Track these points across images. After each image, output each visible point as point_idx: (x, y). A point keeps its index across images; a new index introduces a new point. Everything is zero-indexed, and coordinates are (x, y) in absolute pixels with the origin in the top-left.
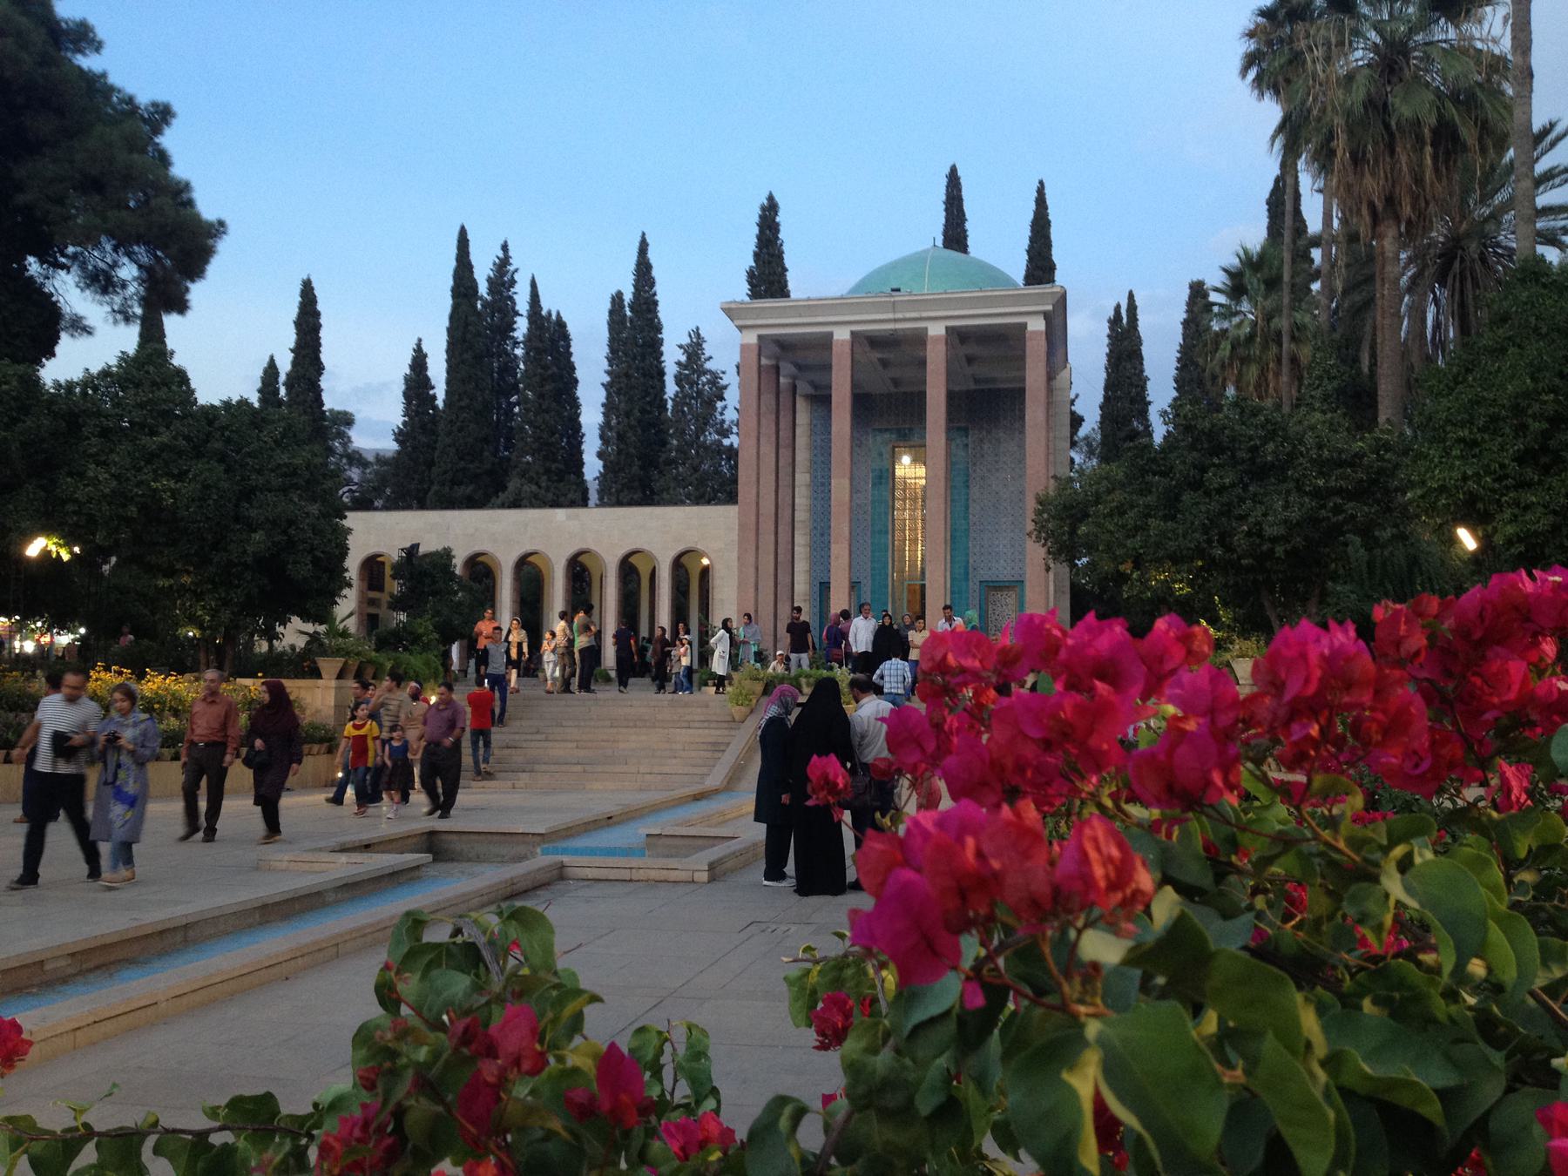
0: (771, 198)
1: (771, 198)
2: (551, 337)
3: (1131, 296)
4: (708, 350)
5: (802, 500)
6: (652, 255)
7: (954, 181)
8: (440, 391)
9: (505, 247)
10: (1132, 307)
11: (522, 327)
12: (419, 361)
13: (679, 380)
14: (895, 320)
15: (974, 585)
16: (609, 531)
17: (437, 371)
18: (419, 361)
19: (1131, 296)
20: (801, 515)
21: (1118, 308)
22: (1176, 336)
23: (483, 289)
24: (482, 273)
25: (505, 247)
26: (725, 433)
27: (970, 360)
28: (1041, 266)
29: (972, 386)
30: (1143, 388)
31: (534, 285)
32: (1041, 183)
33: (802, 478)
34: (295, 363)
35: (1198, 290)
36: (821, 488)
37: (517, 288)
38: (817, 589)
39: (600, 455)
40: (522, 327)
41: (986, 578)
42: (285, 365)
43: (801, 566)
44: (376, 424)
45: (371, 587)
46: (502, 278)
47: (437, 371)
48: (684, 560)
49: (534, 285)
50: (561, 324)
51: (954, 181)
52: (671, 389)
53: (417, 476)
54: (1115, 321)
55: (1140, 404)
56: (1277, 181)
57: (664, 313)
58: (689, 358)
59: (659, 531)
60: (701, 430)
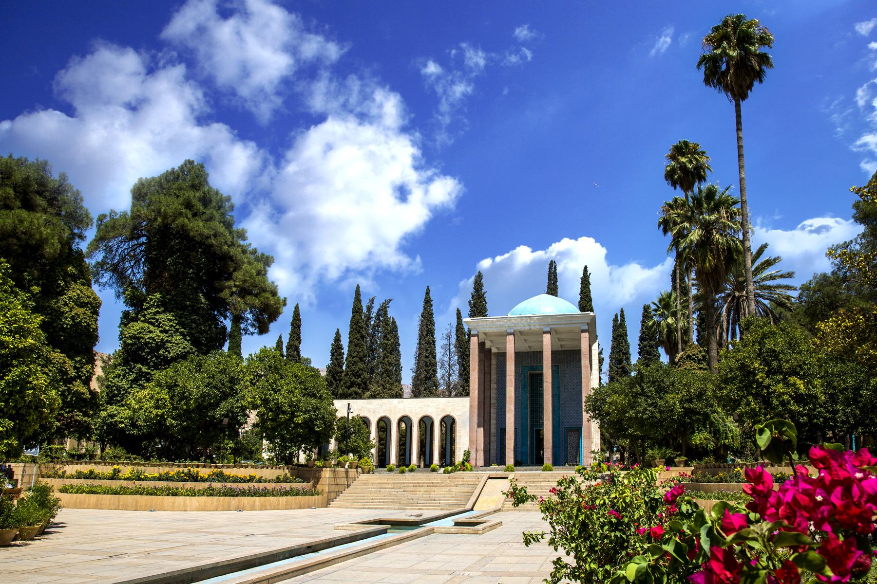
3: (622, 311)
5: (494, 394)
6: (431, 295)
8: (345, 351)
10: (622, 316)
12: (337, 339)
16: (416, 408)
17: (345, 342)
18: (337, 339)
19: (622, 311)
20: (493, 401)
21: (616, 316)
23: (365, 310)
24: (365, 304)
27: (559, 340)
28: (585, 303)
34: (290, 340)
35: (646, 308)
42: (286, 341)
47: (345, 342)
50: (394, 322)
54: (615, 320)
55: (627, 354)
59: (436, 408)
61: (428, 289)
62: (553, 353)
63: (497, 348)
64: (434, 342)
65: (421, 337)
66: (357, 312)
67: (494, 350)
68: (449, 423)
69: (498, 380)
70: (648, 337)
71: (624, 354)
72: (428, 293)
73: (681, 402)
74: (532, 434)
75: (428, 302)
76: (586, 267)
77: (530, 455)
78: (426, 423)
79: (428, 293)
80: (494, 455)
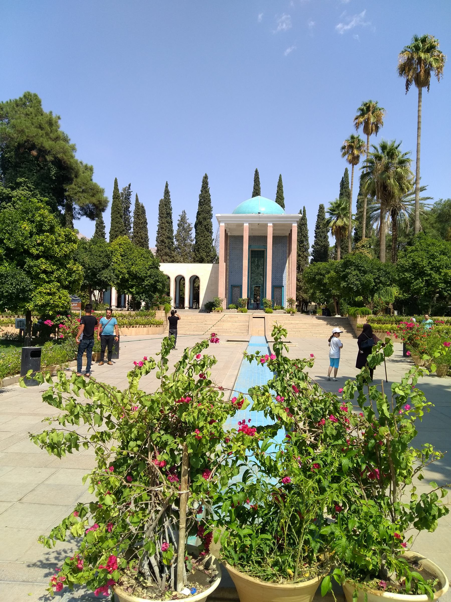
0: (206, 175)
1: (206, 175)
2: (141, 211)
3: (304, 208)
4: (187, 216)
7: (257, 172)
9: (130, 185)
11: (132, 208)
13: (179, 225)
19: (304, 208)
21: (301, 211)
22: (316, 218)
24: (121, 191)
25: (130, 185)
26: (192, 241)
30: (307, 233)
31: (137, 196)
32: (280, 175)
35: (321, 208)
37: (131, 196)
39: (156, 246)
40: (132, 208)
49: (137, 196)
50: (143, 207)
51: (257, 172)
52: (175, 228)
56: (343, 178)
57: (173, 205)
58: (182, 219)
60: (185, 239)
61: (167, 183)
62: (274, 238)
64: (172, 222)
65: (161, 217)
66: (117, 198)
67: (229, 234)
68: (195, 280)
69: (230, 253)
70: (322, 226)
71: (304, 237)
72: (167, 187)
73: (374, 279)
75: (167, 192)
76: (280, 175)
77: (256, 302)
78: (180, 280)
79: (167, 187)
80: (234, 302)
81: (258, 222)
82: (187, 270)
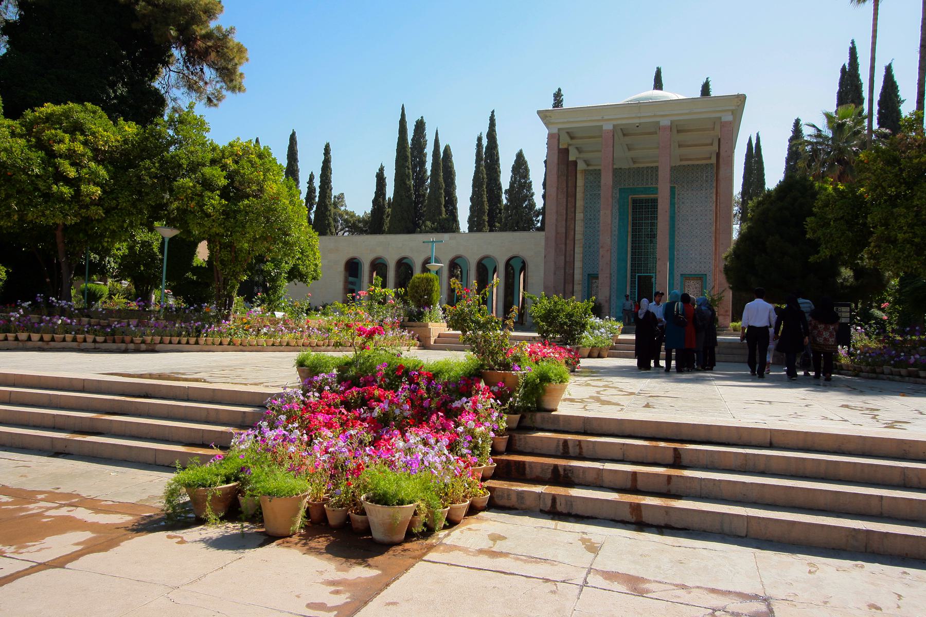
5: (579, 227)
12: (382, 170)
14: (640, 117)
15: (677, 278)
18: (382, 170)
20: (577, 237)
29: (679, 163)
33: (579, 216)
35: (797, 123)
36: (591, 222)
38: (586, 278)
40: (429, 150)
41: (684, 272)
43: (578, 264)
44: (358, 201)
45: (351, 275)
46: (420, 126)
48: (512, 262)
53: (375, 224)
63: (587, 163)
67: (581, 166)
74: (633, 282)
81: (637, 121)
82: (500, 245)
